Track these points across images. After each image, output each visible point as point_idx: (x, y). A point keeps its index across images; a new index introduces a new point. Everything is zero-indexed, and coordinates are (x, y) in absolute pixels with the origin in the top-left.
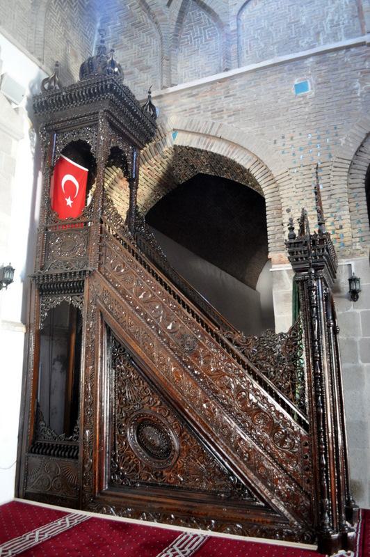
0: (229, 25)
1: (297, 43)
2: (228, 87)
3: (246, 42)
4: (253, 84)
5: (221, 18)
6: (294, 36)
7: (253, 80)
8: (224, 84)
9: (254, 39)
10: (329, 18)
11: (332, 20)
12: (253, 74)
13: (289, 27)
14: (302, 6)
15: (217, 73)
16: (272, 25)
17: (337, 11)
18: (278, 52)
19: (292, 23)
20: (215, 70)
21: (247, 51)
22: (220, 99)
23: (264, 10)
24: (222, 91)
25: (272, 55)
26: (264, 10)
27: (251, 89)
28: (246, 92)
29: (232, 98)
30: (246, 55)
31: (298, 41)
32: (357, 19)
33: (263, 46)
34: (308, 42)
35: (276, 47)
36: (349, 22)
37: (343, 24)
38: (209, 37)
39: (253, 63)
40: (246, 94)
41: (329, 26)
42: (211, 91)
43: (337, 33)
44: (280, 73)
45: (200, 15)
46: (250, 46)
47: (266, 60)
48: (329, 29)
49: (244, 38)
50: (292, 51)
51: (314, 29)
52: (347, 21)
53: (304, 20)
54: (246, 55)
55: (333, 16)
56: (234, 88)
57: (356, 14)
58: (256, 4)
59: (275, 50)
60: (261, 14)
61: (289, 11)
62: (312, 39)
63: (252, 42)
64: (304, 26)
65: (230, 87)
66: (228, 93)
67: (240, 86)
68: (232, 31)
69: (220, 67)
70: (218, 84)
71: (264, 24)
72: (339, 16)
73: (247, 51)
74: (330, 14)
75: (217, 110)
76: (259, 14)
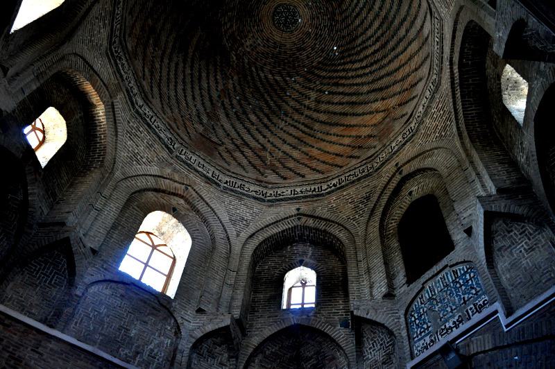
0: (77, 287)
1: (119, 349)
2: (40, 341)
3: (81, 314)
4: (63, 356)
5: (76, 278)
6: (119, 340)
7: (66, 353)
8: (40, 337)
9: (88, 316)
10: (151, 347)
11: (152, 350)
12: (69, 347)
13: (119, 329)
14: (137, 320)
15: (40, 321)
16: (108, 317)
17: (158, 346)
18: (100, 345)
19: (124, 328)
20: (40, 317)
21: (76, 323)
22: (27, 348)
23: (109, 299)
24: (33, 341)
25: (93, 343)
26: (109, 299)
27: (59, 360)
28: (54, 360)
29: (36, 356)
30: (73, 325)
31: (120, 347)
32: (168, 363)
33: (92, 328)
34: (126, 354)
35: (101, 338)
36: (162, 362)
37: (158, 360)
38: (54, 283)
39: (75, 337)
40: (52, 362)
41: (148, 353)
42: (23, 332)
43: (150, 364)
44: (91, 364)
45: (62, 260)
46: (82, 320)
47: (87, 344)
48: (147, 356)
49: (81, 309)
50: (111, 353)
51: (136, 346)
52: (161, 360)
53: (133, 333)
54: (73, 325)
55: (155, 348)
56: (45, 347)
57: (170, 359)
58: (106, 288)
59: (99, 341)
60: (105, 300)
61: (127, 316)
62: (131, 355)
63: (85, 318)
64: (131, 338)
65: (43, 343)
66: (37, 348)
67: (51, 350)
68: (76, 295)
69: (46, 319)
70: (34, 332)
71: (103, 310)
72: (159, 350)
73: (76, 323)
74: (153, 344)
75: (16, 357)
76: (103, 298)
